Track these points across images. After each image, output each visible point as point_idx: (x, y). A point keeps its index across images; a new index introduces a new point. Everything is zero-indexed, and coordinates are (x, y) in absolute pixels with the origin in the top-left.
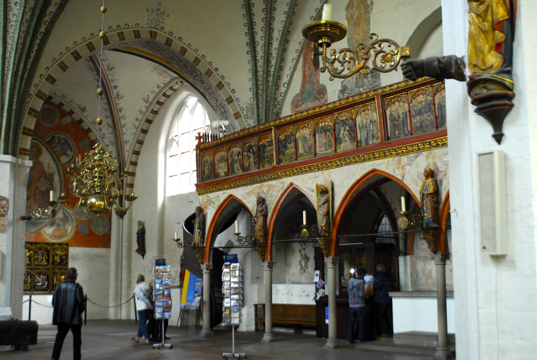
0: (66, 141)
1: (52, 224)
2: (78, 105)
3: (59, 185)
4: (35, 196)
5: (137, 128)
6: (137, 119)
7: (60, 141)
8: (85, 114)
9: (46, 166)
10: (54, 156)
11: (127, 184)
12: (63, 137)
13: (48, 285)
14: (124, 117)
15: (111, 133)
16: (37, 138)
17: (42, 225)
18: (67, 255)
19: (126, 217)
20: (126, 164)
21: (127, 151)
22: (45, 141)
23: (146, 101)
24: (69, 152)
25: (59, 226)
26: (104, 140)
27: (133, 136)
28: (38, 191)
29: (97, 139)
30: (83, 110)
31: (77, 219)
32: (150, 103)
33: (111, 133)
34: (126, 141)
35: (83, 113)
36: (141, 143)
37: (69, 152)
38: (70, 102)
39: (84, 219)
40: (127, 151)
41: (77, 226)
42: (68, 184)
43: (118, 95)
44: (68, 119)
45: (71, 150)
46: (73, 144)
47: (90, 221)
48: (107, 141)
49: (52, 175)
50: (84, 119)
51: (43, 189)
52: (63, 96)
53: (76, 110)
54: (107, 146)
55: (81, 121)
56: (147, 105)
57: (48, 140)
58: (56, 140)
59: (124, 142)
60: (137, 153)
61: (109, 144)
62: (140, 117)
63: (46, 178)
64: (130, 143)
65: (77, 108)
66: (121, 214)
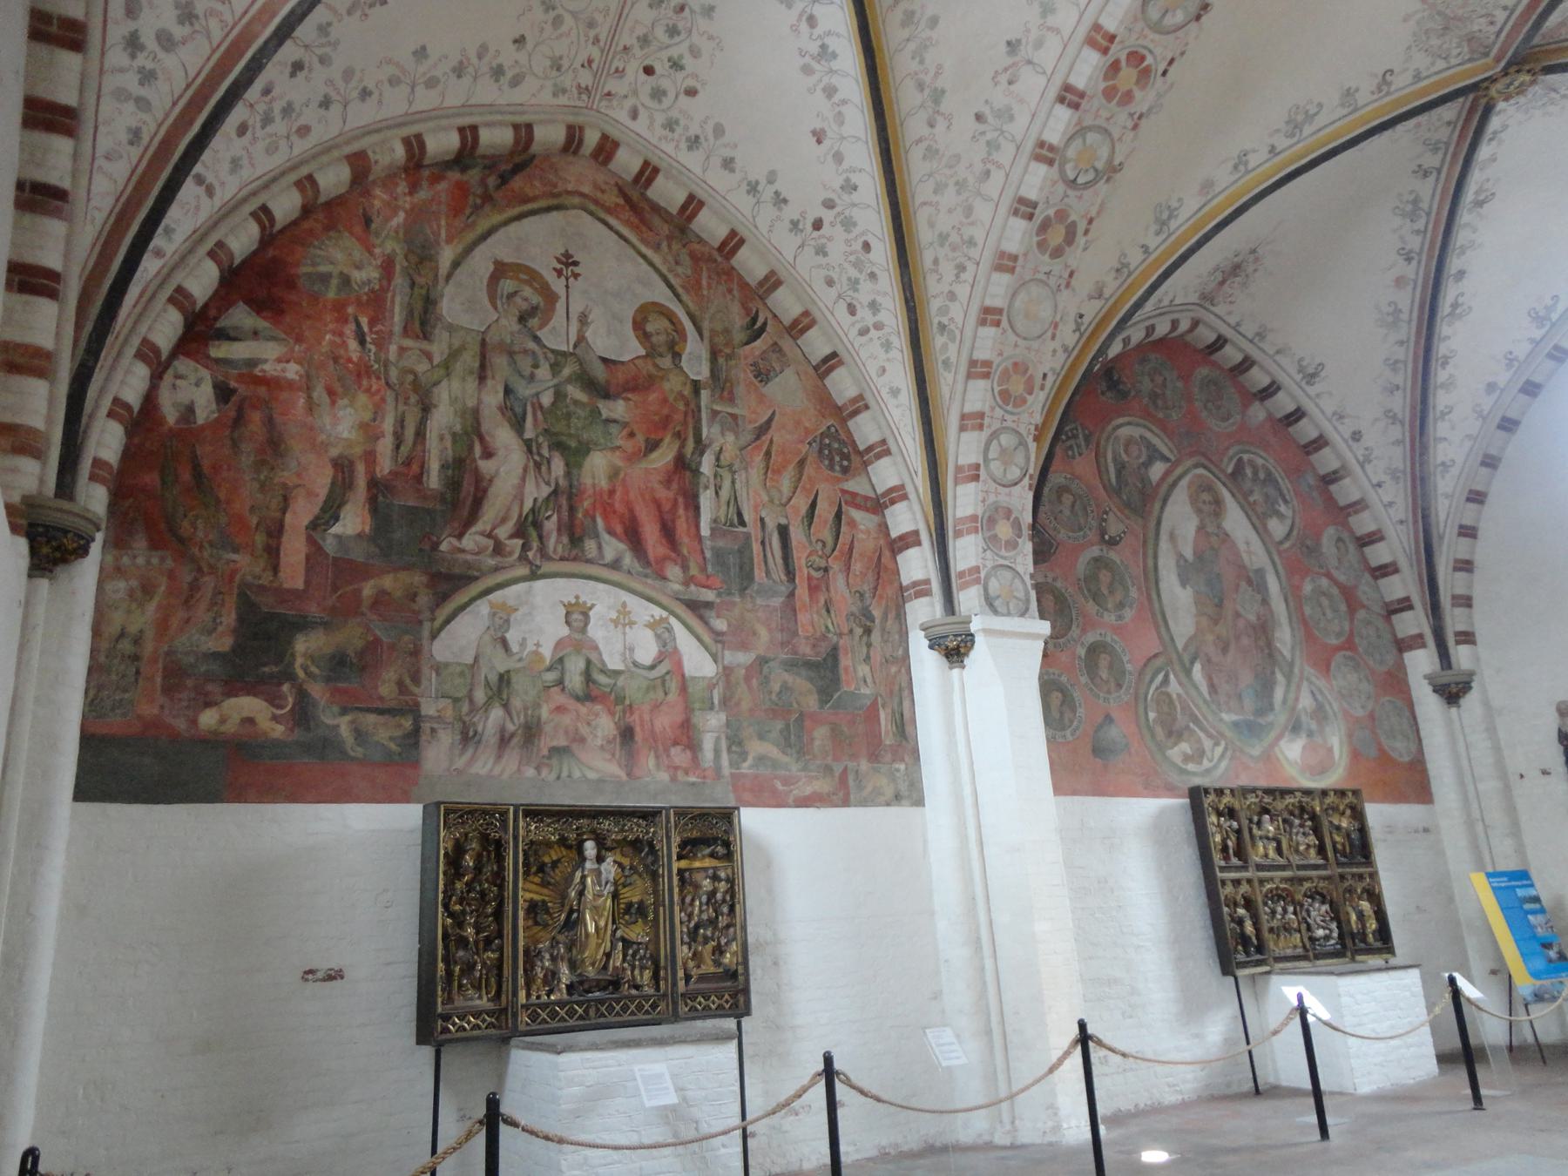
0: (1269, 474)
1: (1296, 728)
2: (1301, 359)
3: (1283, 606)
4: (1238, 638)
5: (1484, 419)
6: (1491, 387)
7: (1255, 473)
8: (1311, 390)
9: (1242, 547)
10: (1254, 519)
11: (1454, 597)
12: (1260, 461)
13: (1341, 936)
14: (1448, 385)
15: (1398, 442)
16: (1207, 463)
17: (1273, 735)
18: (1363, 830)
19: (1471, 701)
20: (1441, 538)
21: (1447, 496)
22: (1223, 471)
23: (1539, 319)
24: (1282, 508)
25: (1310, 734)
26: (1367, 467)
27: (1468, 444)
28: (1241, 623)
29: (1343, 467)
30: (1311, 378)
31: (1346, 713)
32: (1553, 325)
33: (1398, 442)
34: (1443, 464)
35: (1308, 388)
36: (1490, 462)
37: (1282, 508)
38: (1278, 352)
39: (1360, 713)
40: (1447, 496)
41: (1350, 736)
42: (1301, 607)
43: (1455, 305)
44: (1258, 413)
45: (1286, 502)
46: (1285, 484)
47: (1372, 716)
48: (1376, 471)
49: (1260, 572)
50: (1309, 406)
51: (1252, 618)
52: (1261, 335)
53: (1289, 377)
54: (1379, 485)
55: (1297, 415)
56: (1538, 334)
57: (1230, 470)
58: (1249, 471)
59: (1436, 467)
60: (1477, 497)
61: (1384, 478)
62: (1503, 378)
63: (1250, 582)
64: (1455, 471)
65: (1293, 371)
66: (1452, 692)
